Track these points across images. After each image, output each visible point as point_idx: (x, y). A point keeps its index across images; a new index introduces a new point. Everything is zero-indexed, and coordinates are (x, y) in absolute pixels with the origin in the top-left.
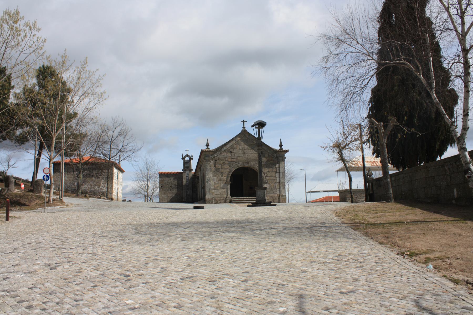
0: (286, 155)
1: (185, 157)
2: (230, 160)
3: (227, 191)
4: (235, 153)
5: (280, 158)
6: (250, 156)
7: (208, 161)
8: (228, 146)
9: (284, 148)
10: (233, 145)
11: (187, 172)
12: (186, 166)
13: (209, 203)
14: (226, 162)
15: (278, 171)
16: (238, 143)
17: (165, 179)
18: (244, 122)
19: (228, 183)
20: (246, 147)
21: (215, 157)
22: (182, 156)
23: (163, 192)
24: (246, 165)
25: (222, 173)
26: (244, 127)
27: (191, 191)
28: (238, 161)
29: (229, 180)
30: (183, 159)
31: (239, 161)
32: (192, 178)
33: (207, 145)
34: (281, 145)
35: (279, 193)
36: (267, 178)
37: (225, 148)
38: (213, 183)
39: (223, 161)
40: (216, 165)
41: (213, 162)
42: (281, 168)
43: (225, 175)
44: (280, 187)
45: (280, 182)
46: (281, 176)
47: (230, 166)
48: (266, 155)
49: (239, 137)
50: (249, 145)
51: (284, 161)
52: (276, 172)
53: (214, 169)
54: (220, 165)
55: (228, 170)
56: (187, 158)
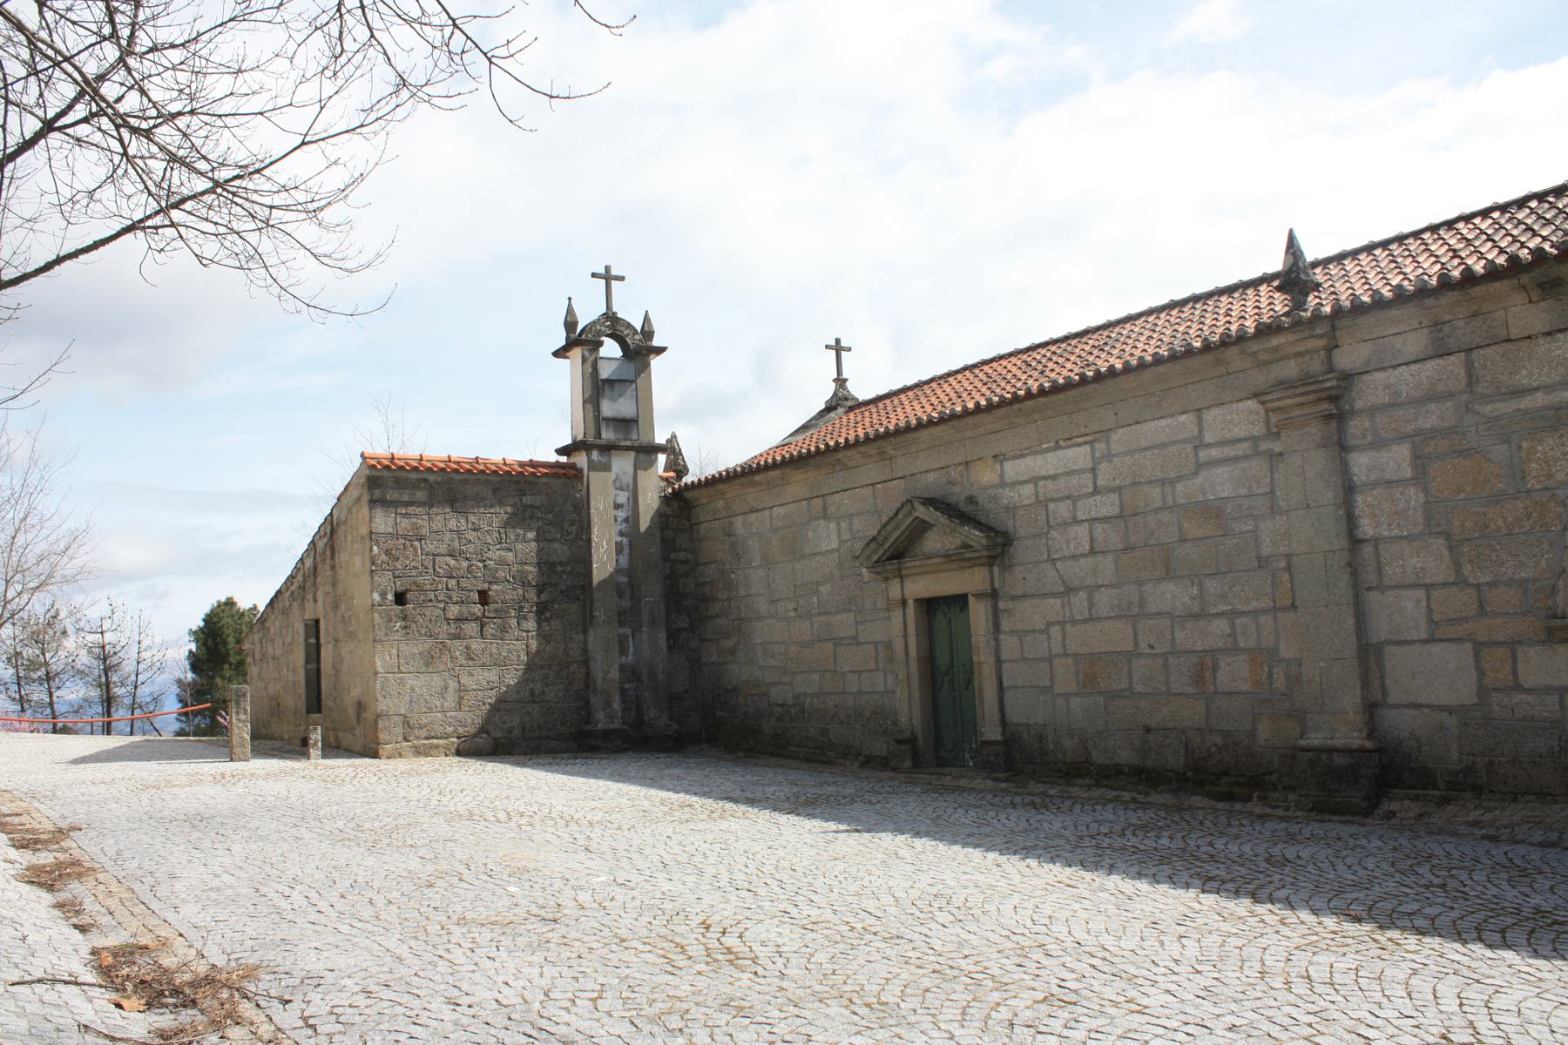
11: (622, 464)
12: (608, 408)
22: (570, 325)
32: (661, 518)
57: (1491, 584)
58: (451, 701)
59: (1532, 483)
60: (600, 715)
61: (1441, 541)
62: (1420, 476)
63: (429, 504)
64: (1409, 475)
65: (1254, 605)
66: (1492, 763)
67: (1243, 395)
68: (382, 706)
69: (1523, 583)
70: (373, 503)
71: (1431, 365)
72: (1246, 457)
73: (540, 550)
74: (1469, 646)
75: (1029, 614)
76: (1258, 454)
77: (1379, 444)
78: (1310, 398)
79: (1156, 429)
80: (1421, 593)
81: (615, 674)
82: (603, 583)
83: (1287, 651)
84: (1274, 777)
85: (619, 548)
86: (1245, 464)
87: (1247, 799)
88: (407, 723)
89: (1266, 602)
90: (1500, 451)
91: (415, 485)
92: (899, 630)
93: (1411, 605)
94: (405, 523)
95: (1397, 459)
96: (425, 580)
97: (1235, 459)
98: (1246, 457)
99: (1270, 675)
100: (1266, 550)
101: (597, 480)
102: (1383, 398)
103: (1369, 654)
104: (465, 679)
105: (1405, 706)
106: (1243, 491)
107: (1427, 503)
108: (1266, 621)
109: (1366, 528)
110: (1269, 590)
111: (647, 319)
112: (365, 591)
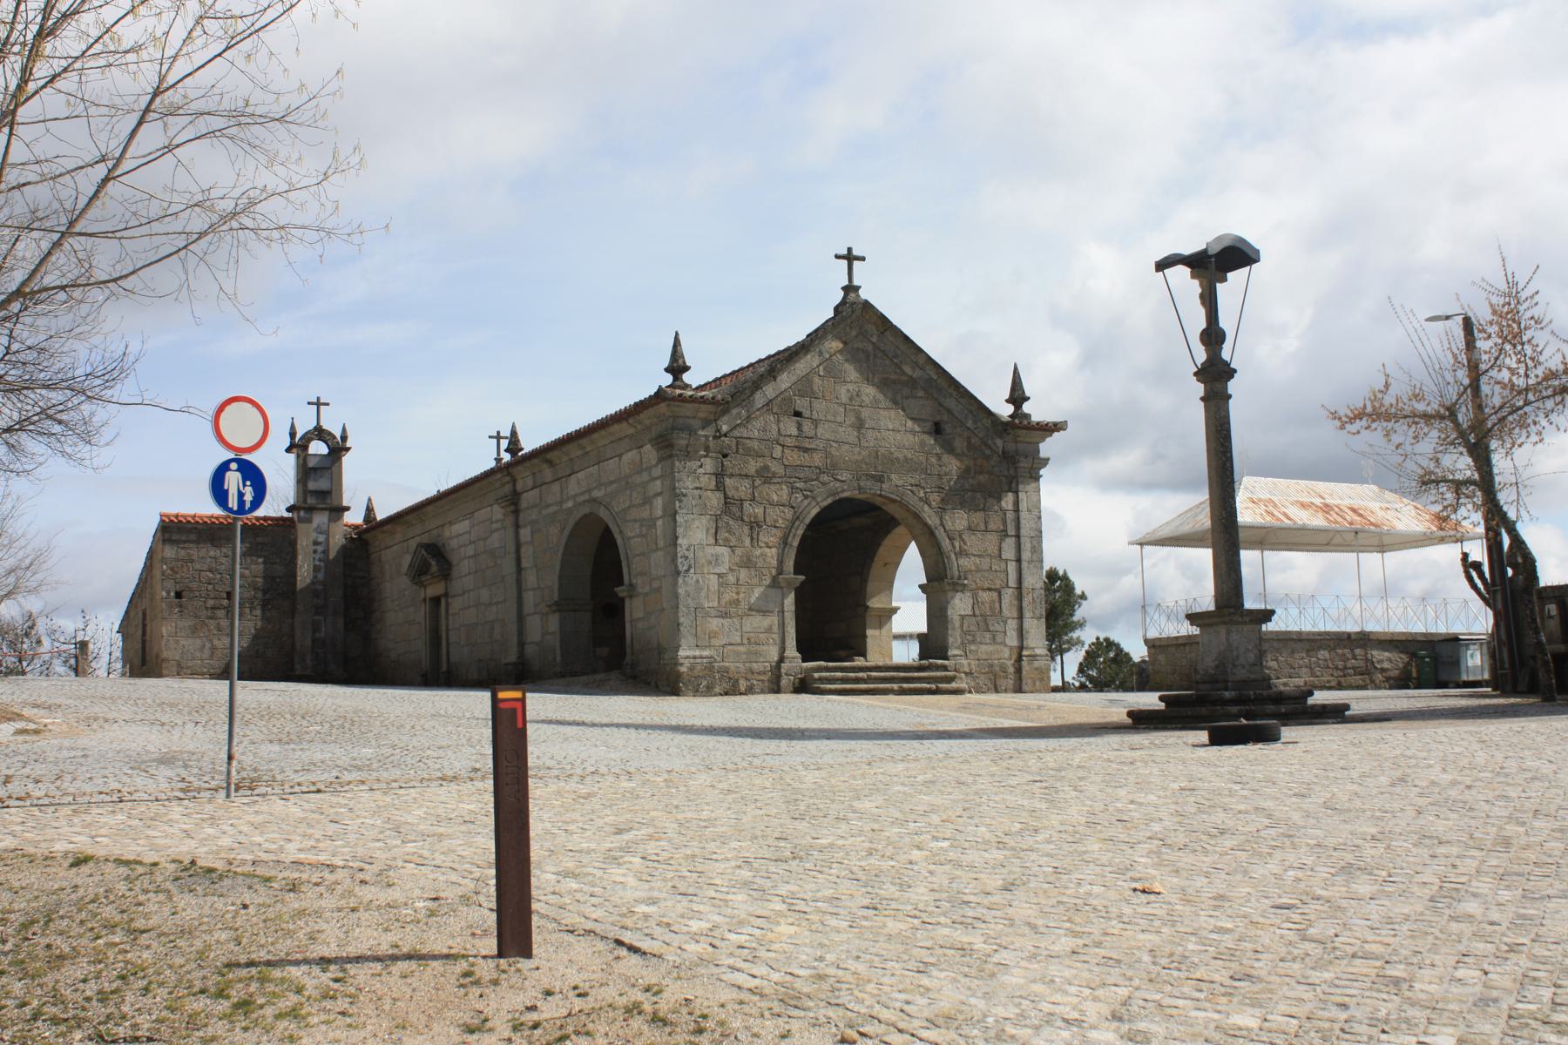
0: (1047, 448)
1: (307, 438)
2: (793, 457)
3: (782, 625)
4: (816, 423)
5: (1024, 464)
6: (878, 438)
7: (688, 455)
8: (785, 380)
9: (1036, 410)
10: (806, 379)
11: (320, 519)
12: (312, 485)
13: (696, 692)
14: (775, 467)
15: (1011, 531)
16: (832, 372)
17: (194, 552)
18: (850, 257)
19: (789, 583)
20: (869, 391)
21: (719, 435)
22: (293, 434)
23: (187, 623)
24: (870, 490)
25: (755, 525)
26: (850, 289)
27: (341, 622)
28: (831, 468)
29: (790, 564)
30: (298, 446)
31: (834, 466)
32: (345, 551)
33: (677, 367)
34: (1017, 397)
35: (1015, 643)
36: (964, 562)
37: (769, 391)
38: (714, 579)
39: (760, 463)
40: (728, 481)
41: (709, 465)
42: (1024, 515)
43: (770, 537)
44: (1020, 609)
45: (1019, 587)
46: (1026, 555)
47: (793, 489)
48: (959, 444)
49: (838, 337)
50: (884, 385)
51: (1037, 478)
52: (1004, 534)
53: (715, 500)
54: (746, 483)
55: (783, 511)
56: (318, 448)
58: (207, 653)
60: (298, 667)
63: (197, 542)
68: (165, 654)
70: (164, 541)
73: (265, 570)
75: (456, 604)
79: (483, 514)
81: (308, 642)
82: (302, 590)
85: (316, 569)
88: (179, 665)
91: (190, 531)
92: (421, 615)
94: (182, 553)
96: (194, 585)
101: (301, 527)
103: (521, 619)
104: (216, 642)
109: (524, 564)
111: (344, 429)
112: (162, 592)
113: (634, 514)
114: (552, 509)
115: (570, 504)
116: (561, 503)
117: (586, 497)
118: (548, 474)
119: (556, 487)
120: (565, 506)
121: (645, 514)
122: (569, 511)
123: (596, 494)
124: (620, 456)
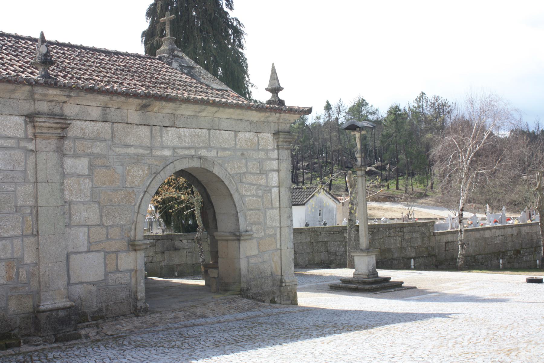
57: (112, 226)
59: (128, 185)
61: (97, 205)
62: (90, 176)
64: (87, 173)
65: (11, 233)
66: (108, 305)
67: (16, 113)
69: (122, 226)
71: (99, 124)
72: (12, 148)
74: (103, 253)
76: (19, 148)
77: (76, 156)
78: (58, 125)
80: (86, 229)
83: (29, 259)
84: (17, 331)
86: (12, 152)
87: (19, 345)
89: (18, 232)
90: (119, 169)
93: (82, 234)
95: (81, 165)
97: (6, 148)
98: (12, 148)
99: (18, 273)
100: (20, 203)
102: (80, 134)
105: (77, 284)
106: (10, 168)
107: (92, 187)
108: (17, 242)
110: (20, 225)
113: (251, 179)
114: (132, 151)
115: (167, 153)
116: (151, 149)
117: (192, 152)
118: (134, 116)
119: (144, 131)
120: (158, 153)
121: (263, 182)
122: (166, 162)
123: (203, 153)
124: (236, 132)
